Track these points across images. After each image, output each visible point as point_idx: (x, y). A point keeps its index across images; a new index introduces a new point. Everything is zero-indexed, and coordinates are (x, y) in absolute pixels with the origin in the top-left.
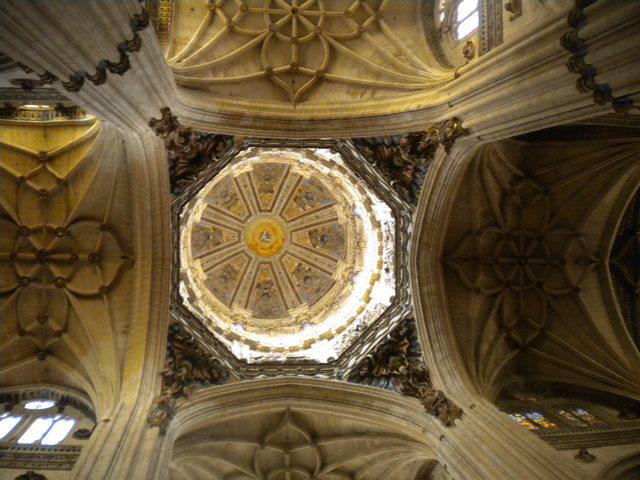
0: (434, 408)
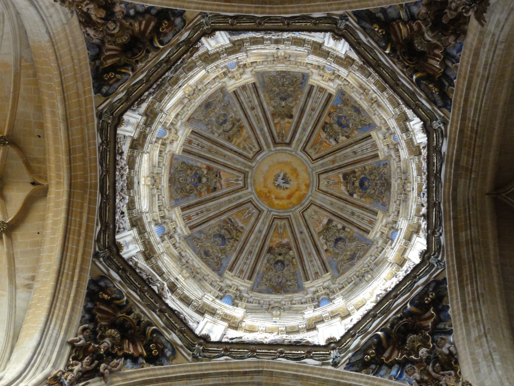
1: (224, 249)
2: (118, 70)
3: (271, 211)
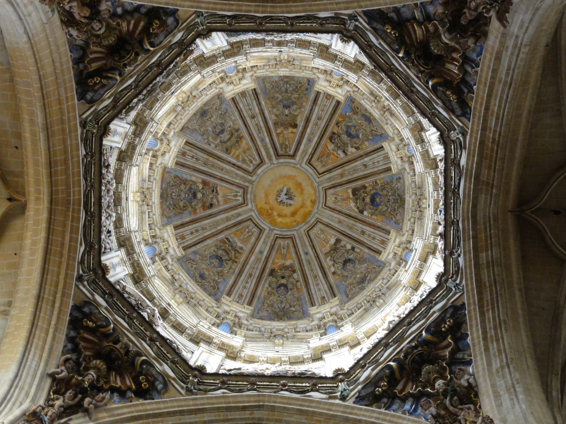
1: (221, 271)
2: (105, 74)
3: (274, 230)
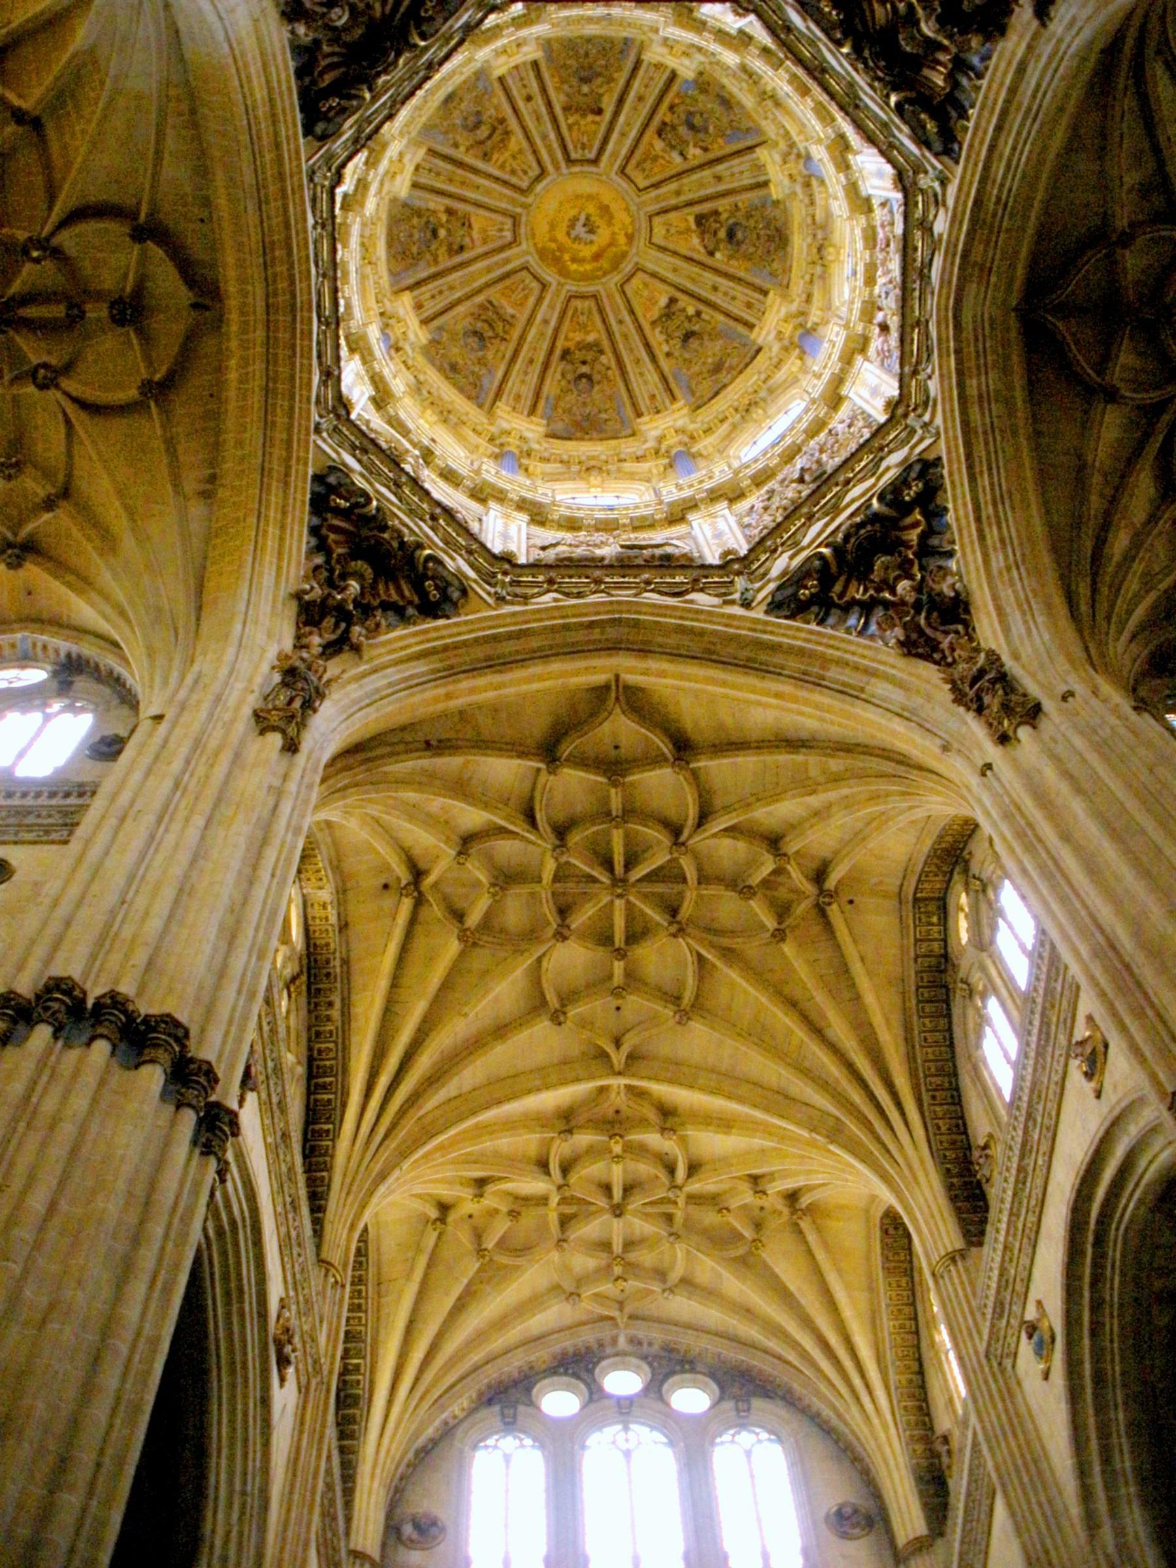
0: (972, 694)
1: (484, 357)
